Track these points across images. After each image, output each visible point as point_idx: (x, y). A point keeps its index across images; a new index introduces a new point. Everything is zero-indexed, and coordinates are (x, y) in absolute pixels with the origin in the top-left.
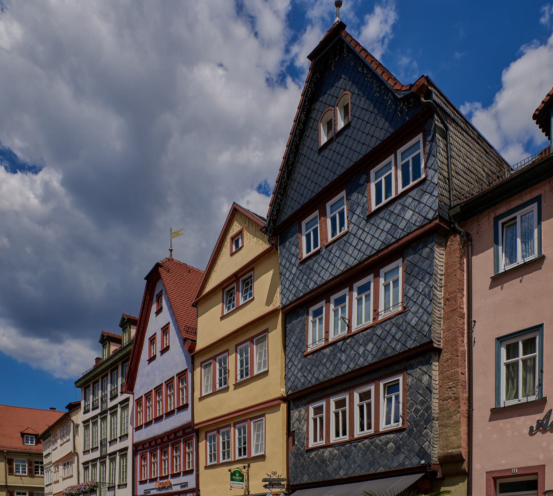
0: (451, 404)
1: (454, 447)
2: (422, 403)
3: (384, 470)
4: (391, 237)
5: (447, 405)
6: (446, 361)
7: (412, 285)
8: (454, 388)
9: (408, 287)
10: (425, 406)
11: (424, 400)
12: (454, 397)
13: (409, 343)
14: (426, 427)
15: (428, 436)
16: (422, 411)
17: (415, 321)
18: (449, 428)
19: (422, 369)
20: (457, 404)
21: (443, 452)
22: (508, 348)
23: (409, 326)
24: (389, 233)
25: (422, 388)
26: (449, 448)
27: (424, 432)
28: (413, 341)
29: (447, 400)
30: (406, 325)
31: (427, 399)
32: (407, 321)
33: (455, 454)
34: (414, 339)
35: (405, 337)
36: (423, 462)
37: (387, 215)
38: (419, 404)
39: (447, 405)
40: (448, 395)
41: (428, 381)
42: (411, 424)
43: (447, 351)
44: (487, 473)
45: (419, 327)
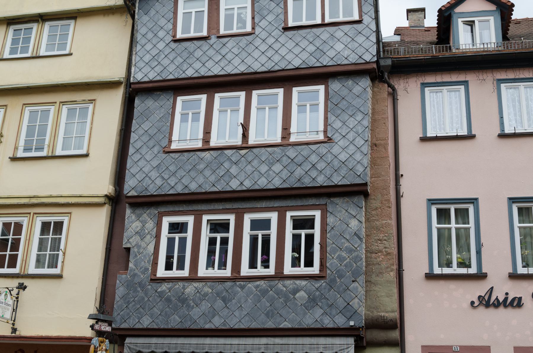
0: (382, 258)
1: (387, 310)
2: (350, 251)
3: (290, 326)
4: (316, 60)
5: (376, 258)
6: (375, 209)
7: (340, 118)
8: (385, 242)
9: (333, 118)
10: (353, 255)
11: (351, 248)
12: (386, 252)
13: (336, 179)
14: (353, 279)
15: (357, 292)
16: (348, 260)
17: (345, 157)
18: (380, 287)
19: (348, 211)
20: (389, 260)
21: (371, 314)
22: (439, 211)
23: (336, 159)
24: (313, 55)
25: (349, 233)
26: (379, 310)
27: (352, 286)
28: (341, 177)
29: (376, 253)
30: (331, 157)
31: (356, 246)
32: (334, 154)
33: (388, 319)
34: (343, 175)
35: (329, 170)
36: (352, 323)
37: (311, 37)
38: (344, 250)
39: (376, 258)
40: (377, 247)
41: (357, 227)
42: (333, 272)
43: (376, 198)
44: (422, 346)
45: (351, 164)
